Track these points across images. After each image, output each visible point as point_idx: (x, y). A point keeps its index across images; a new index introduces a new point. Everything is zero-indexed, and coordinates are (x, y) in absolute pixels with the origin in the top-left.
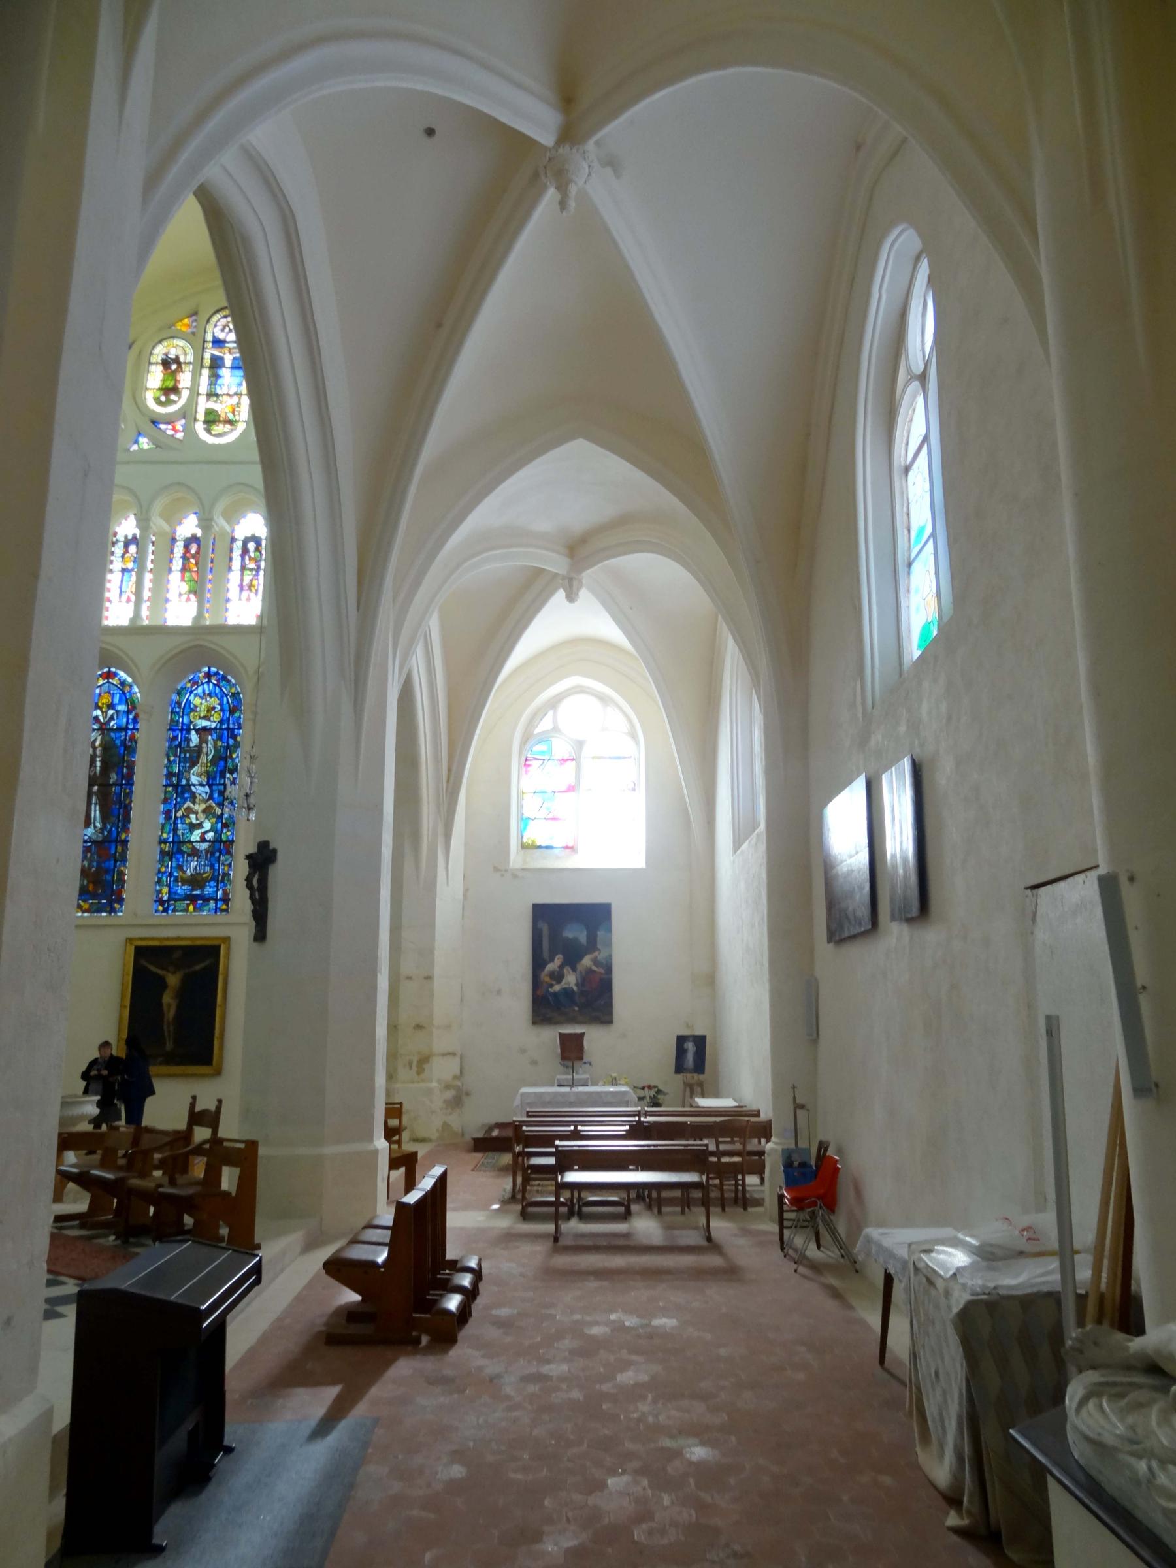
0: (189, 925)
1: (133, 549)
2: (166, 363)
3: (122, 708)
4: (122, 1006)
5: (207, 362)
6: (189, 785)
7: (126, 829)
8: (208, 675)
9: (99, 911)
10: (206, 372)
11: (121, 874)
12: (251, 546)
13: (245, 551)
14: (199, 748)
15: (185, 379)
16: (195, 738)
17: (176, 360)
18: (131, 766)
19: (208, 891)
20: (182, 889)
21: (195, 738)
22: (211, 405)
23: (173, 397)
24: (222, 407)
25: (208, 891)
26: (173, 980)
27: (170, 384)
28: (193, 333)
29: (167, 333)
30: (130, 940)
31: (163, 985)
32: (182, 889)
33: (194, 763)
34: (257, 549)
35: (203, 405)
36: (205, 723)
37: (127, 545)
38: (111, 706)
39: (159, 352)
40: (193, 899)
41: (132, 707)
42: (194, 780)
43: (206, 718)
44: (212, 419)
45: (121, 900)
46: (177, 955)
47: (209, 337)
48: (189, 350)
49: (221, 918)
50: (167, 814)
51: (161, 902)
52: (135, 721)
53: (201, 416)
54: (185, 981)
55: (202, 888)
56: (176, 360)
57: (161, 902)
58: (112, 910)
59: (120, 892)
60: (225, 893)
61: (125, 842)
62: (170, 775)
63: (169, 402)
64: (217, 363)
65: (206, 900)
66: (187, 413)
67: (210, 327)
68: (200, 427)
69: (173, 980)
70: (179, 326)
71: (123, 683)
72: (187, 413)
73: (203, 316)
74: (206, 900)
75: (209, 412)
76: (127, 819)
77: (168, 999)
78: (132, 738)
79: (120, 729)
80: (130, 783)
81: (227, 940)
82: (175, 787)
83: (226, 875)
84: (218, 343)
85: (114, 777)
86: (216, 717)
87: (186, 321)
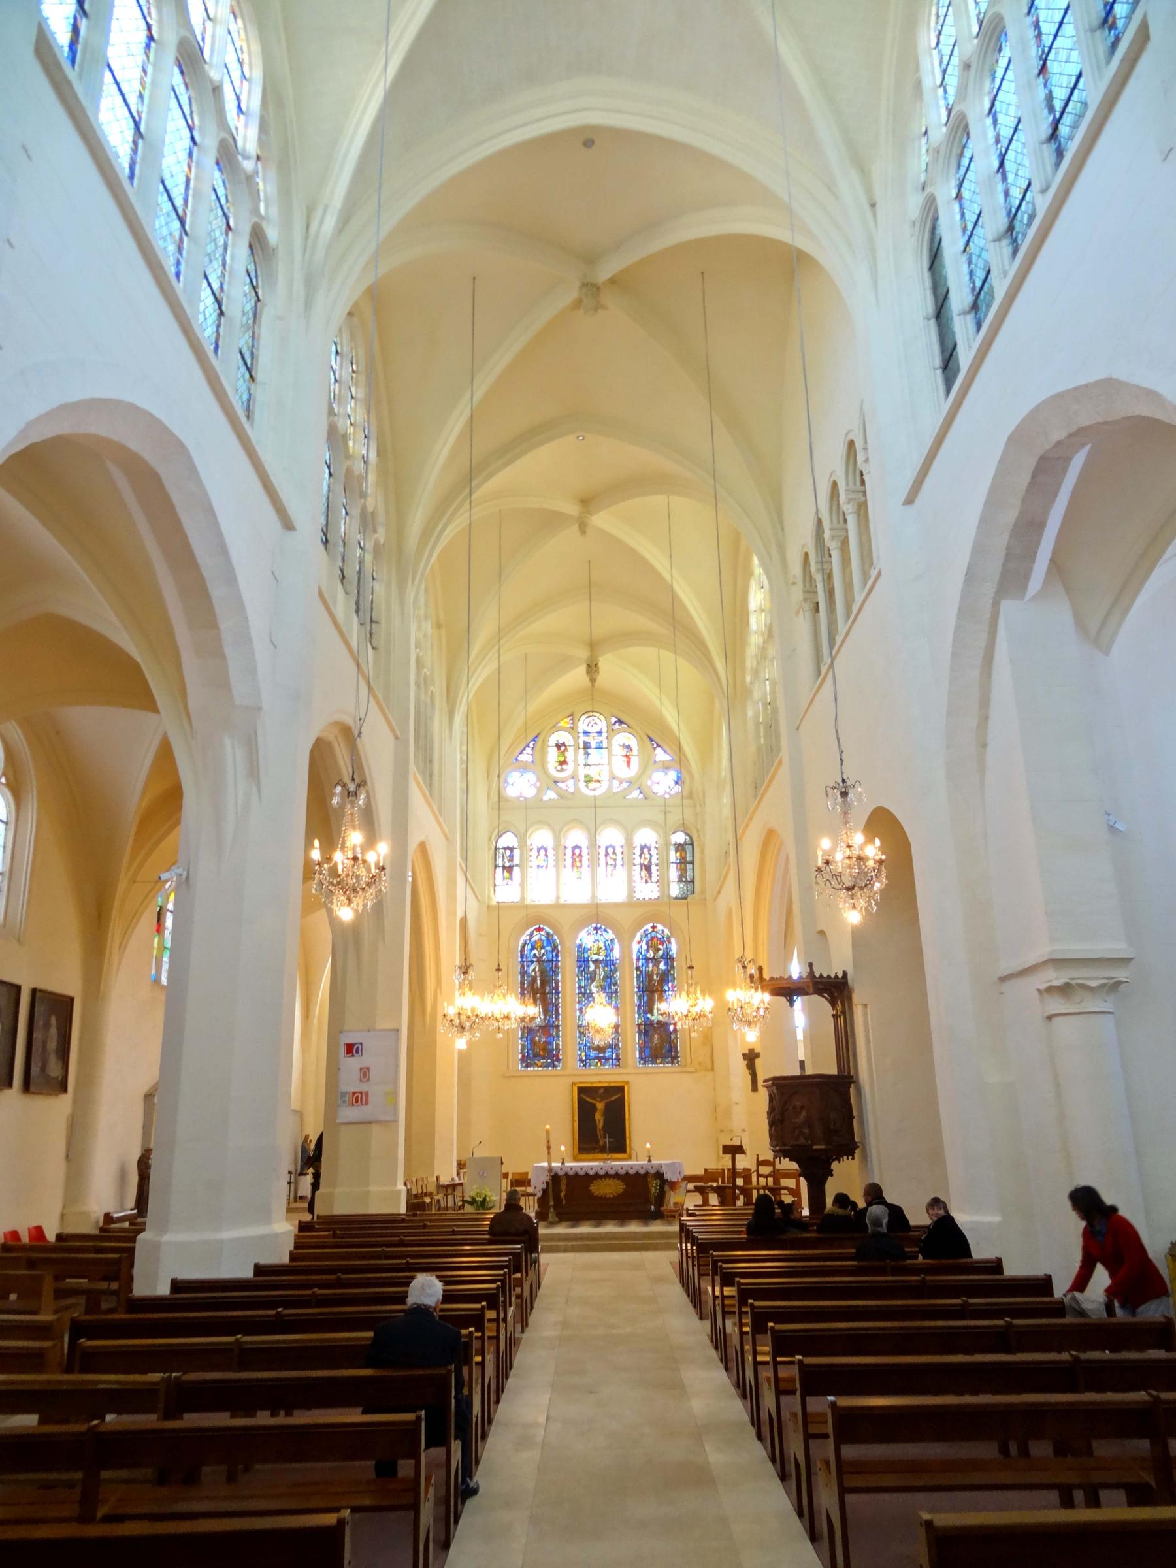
0: (602, 1075)
1: (542, 852)
2: (558, 746)
3: (549, 948)
4: (573, 1121)
5: (581, 745)
6: (591, 993)
7: (557, 1019)
8: (596, 929)
9: (547, 1066)
10: (582, 751)
11: (557, 1045)
12: (610, 850)
13: (607, 854)
14: (595, 971)
15: (570, 755)
16: (592, 967)
17: (564, 744)
18: (557, 983)
19: (607, 1054)
20: (593, 1054)
21: (592, 967)
22: (588, 771)
23: (564, 767)
24: (593, 772)
25: (607, 1054)
26: (600, 1106)
27: (562, 759)
28: (572, 728)
29: (555, 728)
30: (574, 1084)
31: (594, 1108)
32: (593, 1054)
33: (593, 981)
34: (614, 853)
35: (582, 772)
36: (595, 957)
37: (539, 850)
38: (542, 947)
39: (553, 739)
40: (600, 1059)
41: (555, 948)
42: (594, 990)
43: (597, 954)
44: (588, 780)
45: (558, 1060)
46: (602, 1091)
47: (581, 730)
48: (569, 735)
49: (617, 1070)
50: (581, 1010)
51: (581, 1060)
52: (557, 956)
53: (582, 778)
54: (607, 1106)
55: (604, 1052)
56: (564, 744)
57: (581, 1060)
58: (554, 1066)
59: (557, 1056)
60: (618, 1055)
61: (557, 1027)
62: (580, 987)
63: (562, 770)
64: (587, 746)
65: (607, 1059)
66: (573, 777)
67: (580, 723)
68: (582, 785)
69: (600, 1106)
70: (562, 724)
71: (548, 934)
72: (573, 777)
73: (576, 716)
74: (607, 1059)
75: (586, 776)
76: (557, 1014)
77: (599, 1117)
78: (556, 966)
79: (548, 961)
80: (557, 993)
81: (627, 1083)
82: (584, 994)
83: (617, 1045)
84: (586, 733)
85: (548, 990)
86: (603, 953)
87: (567, 720)
